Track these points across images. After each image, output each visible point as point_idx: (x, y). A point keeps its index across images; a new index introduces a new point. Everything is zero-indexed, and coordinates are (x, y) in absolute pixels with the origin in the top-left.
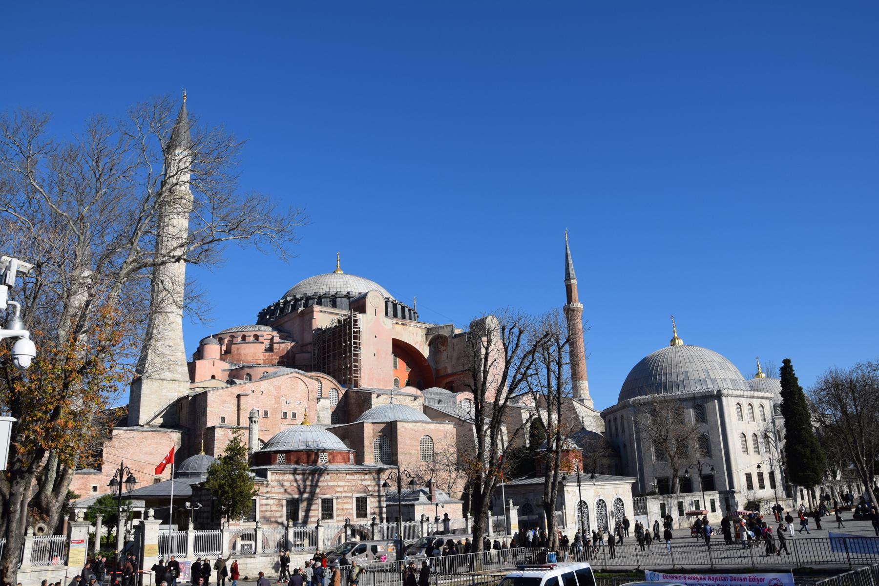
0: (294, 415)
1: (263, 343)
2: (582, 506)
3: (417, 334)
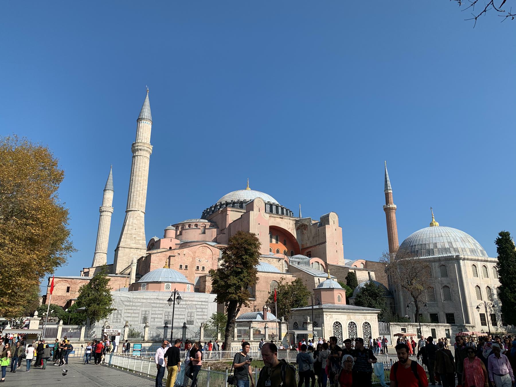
0: (203, 268)
1: (200, 229)
2: (337, 325)
3: (289, 223)
